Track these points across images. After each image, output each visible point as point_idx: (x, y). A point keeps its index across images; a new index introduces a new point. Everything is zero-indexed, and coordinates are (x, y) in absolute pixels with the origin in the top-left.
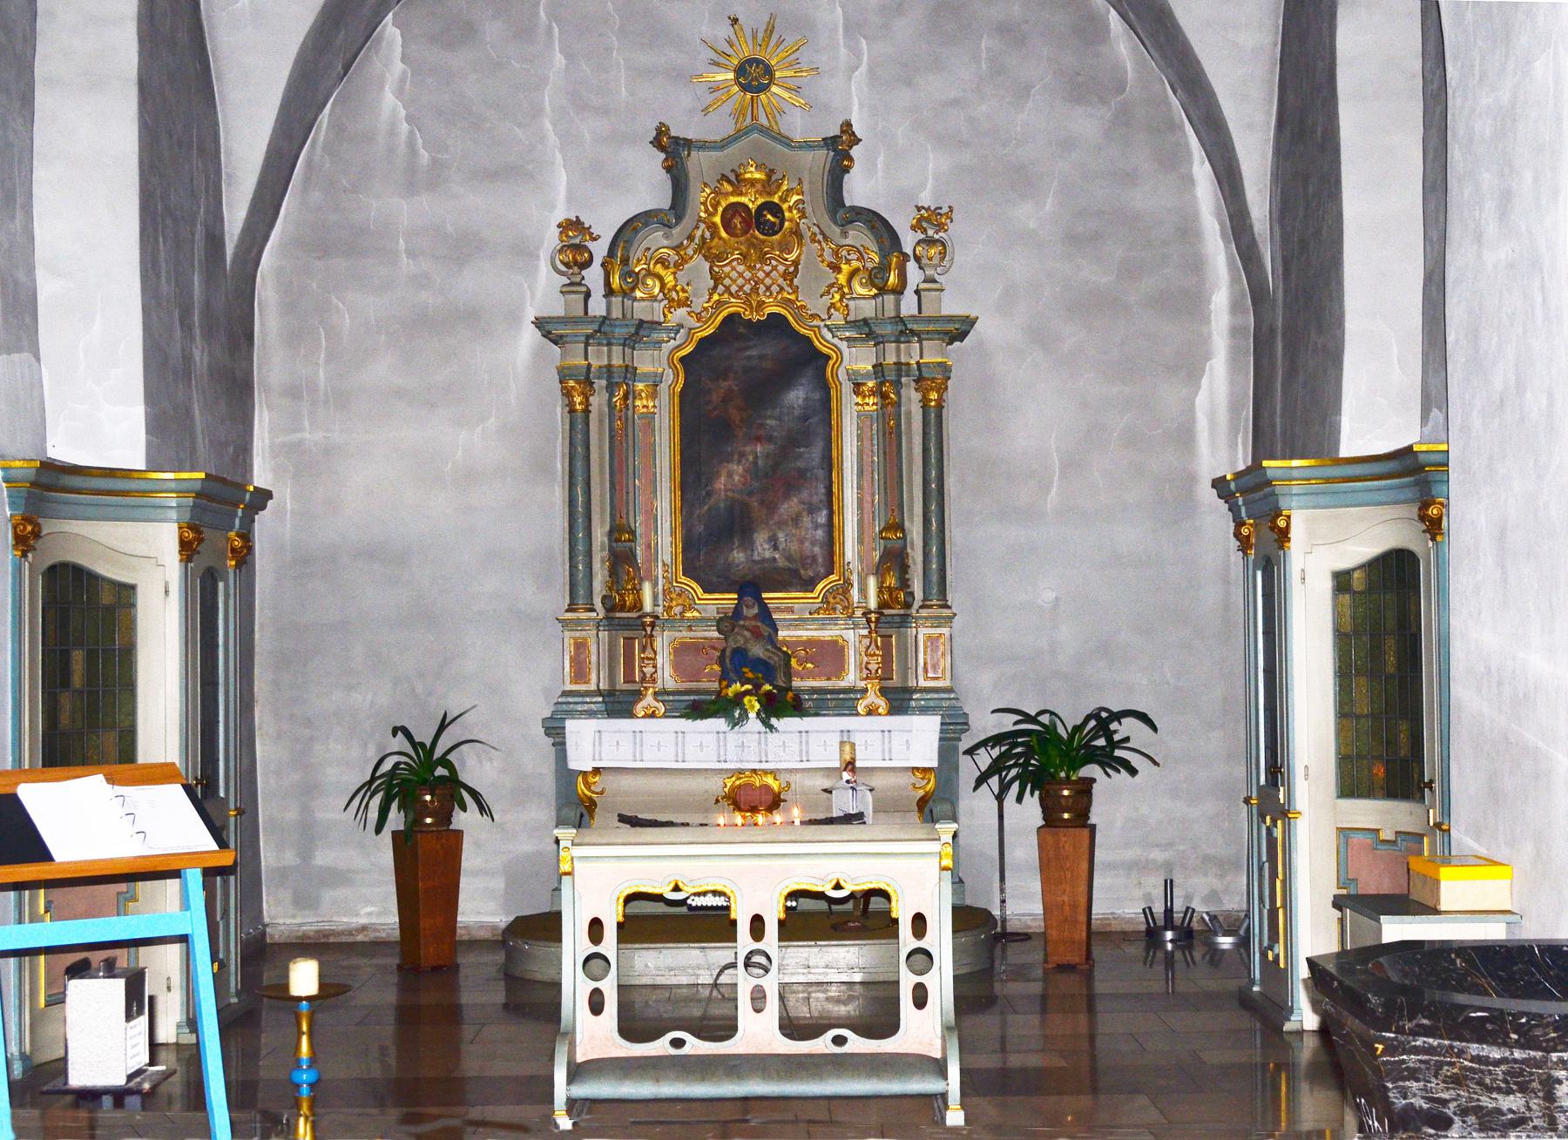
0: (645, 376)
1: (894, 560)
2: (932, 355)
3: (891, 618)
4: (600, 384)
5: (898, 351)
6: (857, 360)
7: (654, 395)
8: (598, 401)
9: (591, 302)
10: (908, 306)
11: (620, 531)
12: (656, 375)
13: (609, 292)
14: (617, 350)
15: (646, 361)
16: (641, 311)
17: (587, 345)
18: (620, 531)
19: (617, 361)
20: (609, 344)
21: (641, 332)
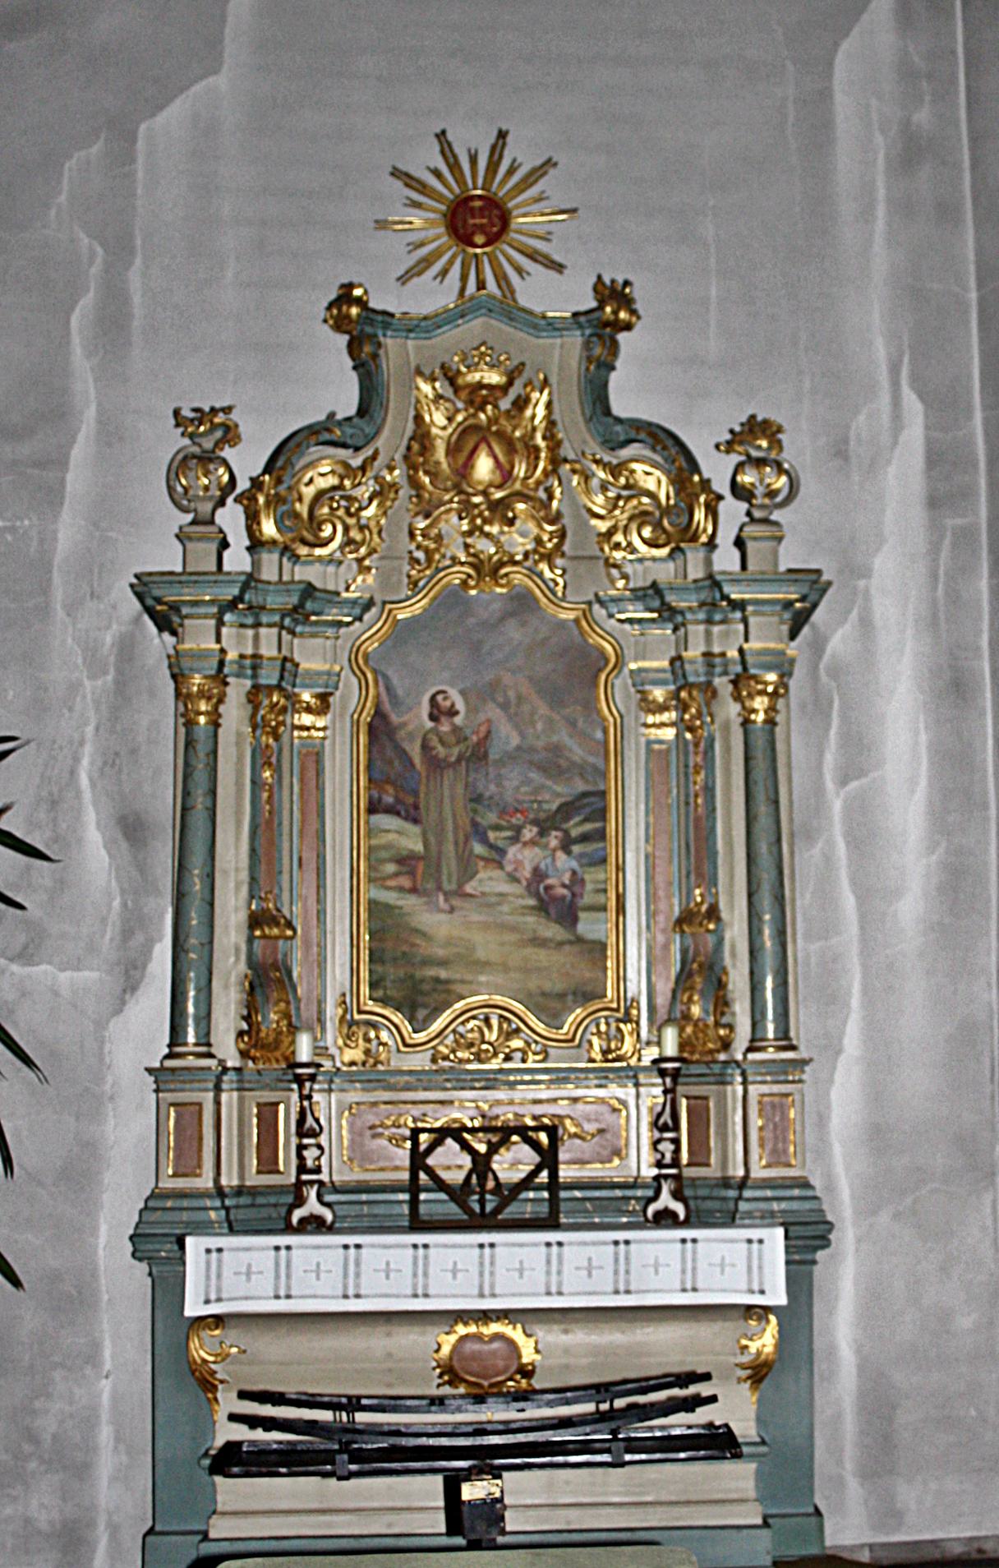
0: (312, 677)
1: (701, 974)
3: (692, 1072)
4: (238, 689)
5: (708, 635)
7: (323, 703)
8: (234, 712)
9: (226, 554)
12: (329, 673)
13: (256, 544)
14: (268, 635)
16: (302, 573)
17: (220, 623)
19: (268, 650)
20: (257, 625)
21: (304, 607)
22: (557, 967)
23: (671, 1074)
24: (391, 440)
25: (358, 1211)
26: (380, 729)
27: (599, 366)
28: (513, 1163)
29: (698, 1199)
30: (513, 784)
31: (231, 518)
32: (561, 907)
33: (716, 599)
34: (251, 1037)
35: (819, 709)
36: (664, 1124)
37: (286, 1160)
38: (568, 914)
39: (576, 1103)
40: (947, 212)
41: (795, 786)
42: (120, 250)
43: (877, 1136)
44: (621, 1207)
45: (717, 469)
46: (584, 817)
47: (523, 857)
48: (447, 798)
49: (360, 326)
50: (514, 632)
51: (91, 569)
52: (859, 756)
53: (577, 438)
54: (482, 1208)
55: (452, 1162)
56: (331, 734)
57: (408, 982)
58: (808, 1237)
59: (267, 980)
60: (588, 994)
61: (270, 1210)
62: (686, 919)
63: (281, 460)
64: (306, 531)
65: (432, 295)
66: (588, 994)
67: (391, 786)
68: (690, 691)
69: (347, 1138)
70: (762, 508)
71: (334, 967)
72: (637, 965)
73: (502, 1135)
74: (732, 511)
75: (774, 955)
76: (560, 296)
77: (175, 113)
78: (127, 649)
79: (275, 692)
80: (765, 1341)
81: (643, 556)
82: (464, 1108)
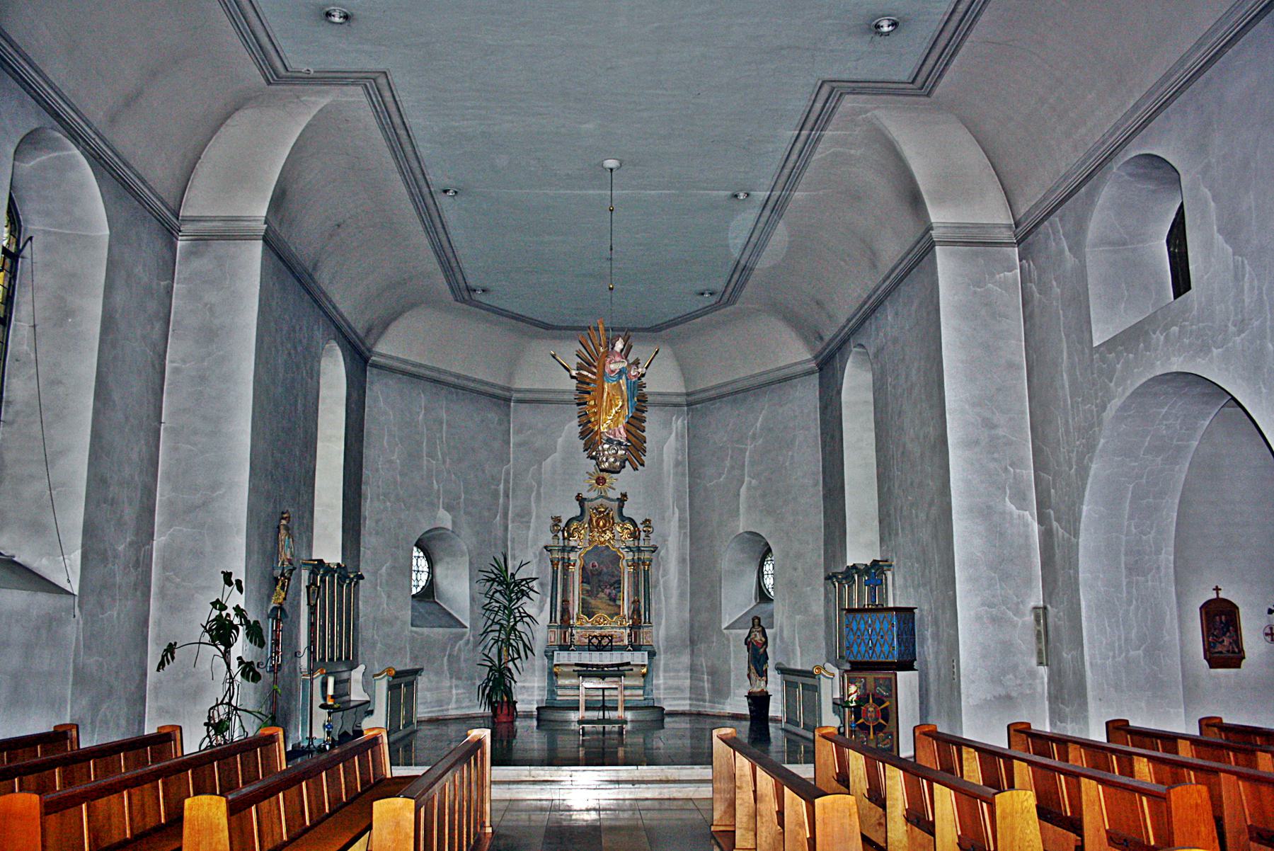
1: (636, 611)
2: (646, 556)
3: (636, 627)
6: (629, 556)
10: (642, 544)
11: (565, 601)
15: (573, 556)
16: (572, 543)
18: (565, 601)
21: (573, 549)
22: (612, 610)
23: (631, 627)
24: (586, 519)
25: (581, 648)
26: (583, 569)
27: (621, 508)
28: (605, 641)
29: (636, 648)
30: (605, 578)
31: (560, 534)
32: (614, 599)
33: (639, 550)
34: (562, 619)
35: (659, 565)
36: (630, 635)
37: (568, 639)
38: (614, 600)
39: (617, 632)
40: (683, 475)
41: (652, 580)
42: (539, 487)
43: (667, 639)
44: (623, 648)
45: (641, 527)
46: (617, 584)
47: (607, 591)
48: (595, 580)
49: (581, 500)
50: (606, 553)
51: (535, 541)
52: (666, 573)
53: (617, 520)
54: (600, 648)
55: (594, 640)
56: (576, 572)
57: (588, 611)
58: (652, 654)
59: (565, 611)
60: (618, 614)
61: (564, 648)
62: (634, 602)
63: (567, 524)
64: (571, 535)
65: (593, 495)
66: (618, 614)
67: (585, 579)
68: (635, 564)
69: (578, 635)
70: (648, 533)
71: (575, 608)
72: (626, 609)
73: (603, 637)
74: (643, 534)
75: (648, 609)
76: (615, 494)
77: (549, 460)
78: (541, 553)
79: (567, 564)
80: (644, 670)
81: (630, 542)
82: (597, 632)
